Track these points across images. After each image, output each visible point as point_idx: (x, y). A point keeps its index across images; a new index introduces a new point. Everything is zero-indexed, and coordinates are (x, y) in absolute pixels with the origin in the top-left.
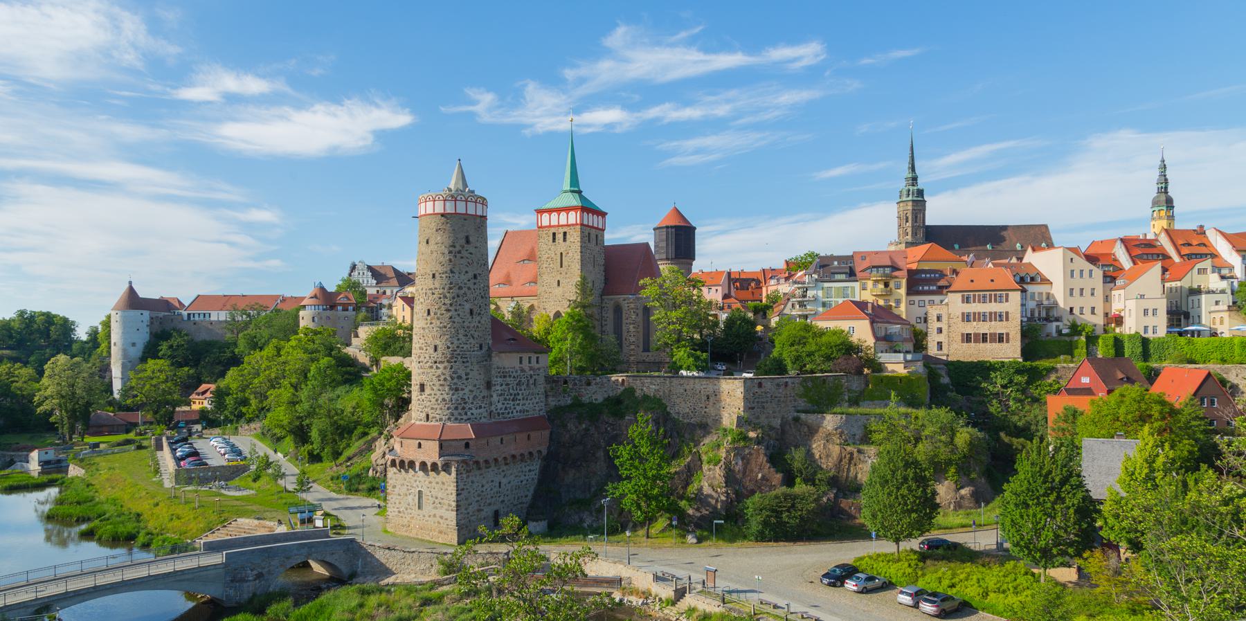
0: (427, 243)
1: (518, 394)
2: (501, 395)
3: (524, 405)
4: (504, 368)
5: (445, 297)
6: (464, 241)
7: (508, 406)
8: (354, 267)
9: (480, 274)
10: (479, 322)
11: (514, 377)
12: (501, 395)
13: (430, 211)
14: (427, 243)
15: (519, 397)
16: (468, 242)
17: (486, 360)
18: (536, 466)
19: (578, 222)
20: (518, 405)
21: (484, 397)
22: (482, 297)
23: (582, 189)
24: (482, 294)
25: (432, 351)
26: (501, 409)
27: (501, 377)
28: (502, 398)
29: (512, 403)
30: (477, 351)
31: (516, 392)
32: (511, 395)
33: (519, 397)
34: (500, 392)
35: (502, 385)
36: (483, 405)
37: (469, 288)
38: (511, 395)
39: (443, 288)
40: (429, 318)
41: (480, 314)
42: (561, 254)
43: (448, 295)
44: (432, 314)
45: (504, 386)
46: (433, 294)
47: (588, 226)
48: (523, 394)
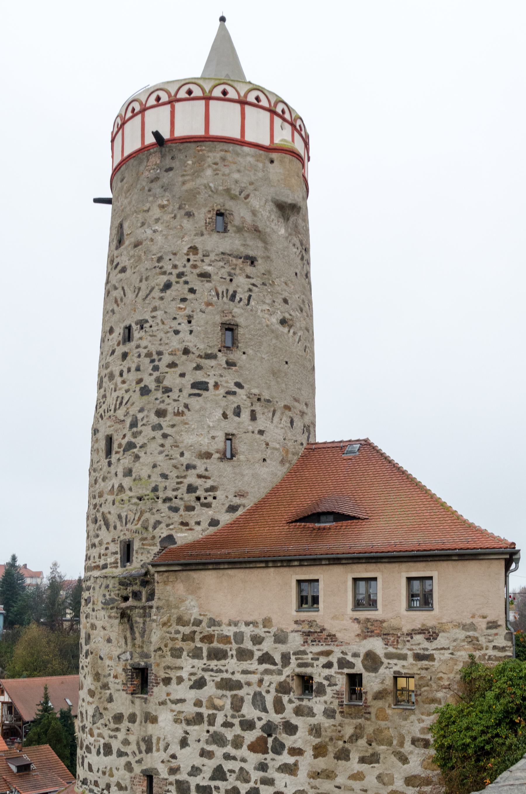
1: (291, 729)
2: (198, 719)
3: (329, 775)
4: (213, 623)
7: (227, 765)
9: (142, 324)
10: (128, 473)
11: (266, 658)
12: (198, 719)
15: (289, 741)
17: (136, 595)
20: (286, 769)
21: (118, 718)
22: (145, 391)
24: (149, 382)
26: (195, 771)
27: (196, 654)
28: (196, 731)
29: (254, 758)
30: (115, 564)
31: (276, 718)
32: (248, 725)
33: (289, 741)
34: (189, 709)
35: (200, 684)
36: (116, 745)
38: (248, 725)
41: (131, 446)
45: (210, 689)
48: (316, 730)
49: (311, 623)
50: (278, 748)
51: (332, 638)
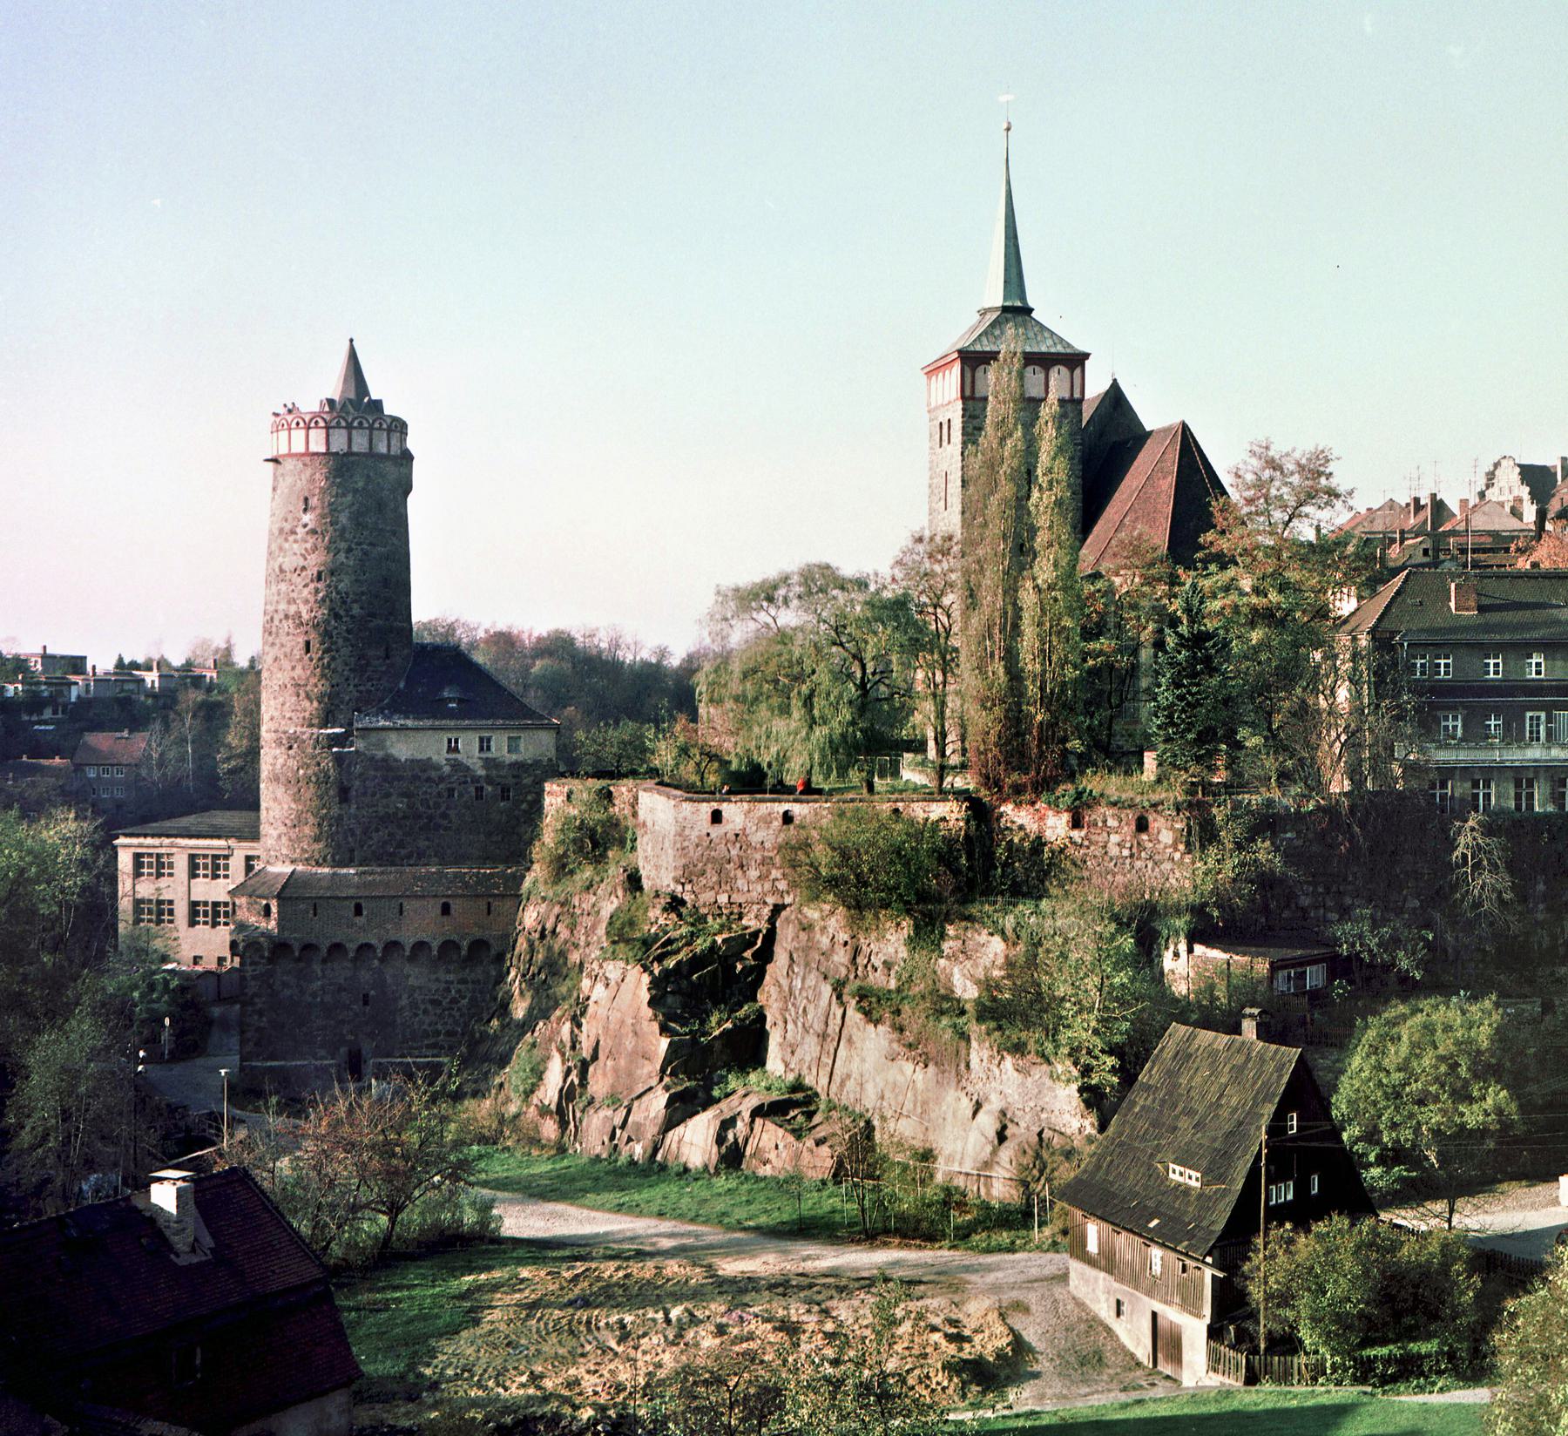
16: (305, 510)
23: (1031, 303)
37: (306, 602)
49: (456, 760)
50: (438, 827)
51: (468, 768)
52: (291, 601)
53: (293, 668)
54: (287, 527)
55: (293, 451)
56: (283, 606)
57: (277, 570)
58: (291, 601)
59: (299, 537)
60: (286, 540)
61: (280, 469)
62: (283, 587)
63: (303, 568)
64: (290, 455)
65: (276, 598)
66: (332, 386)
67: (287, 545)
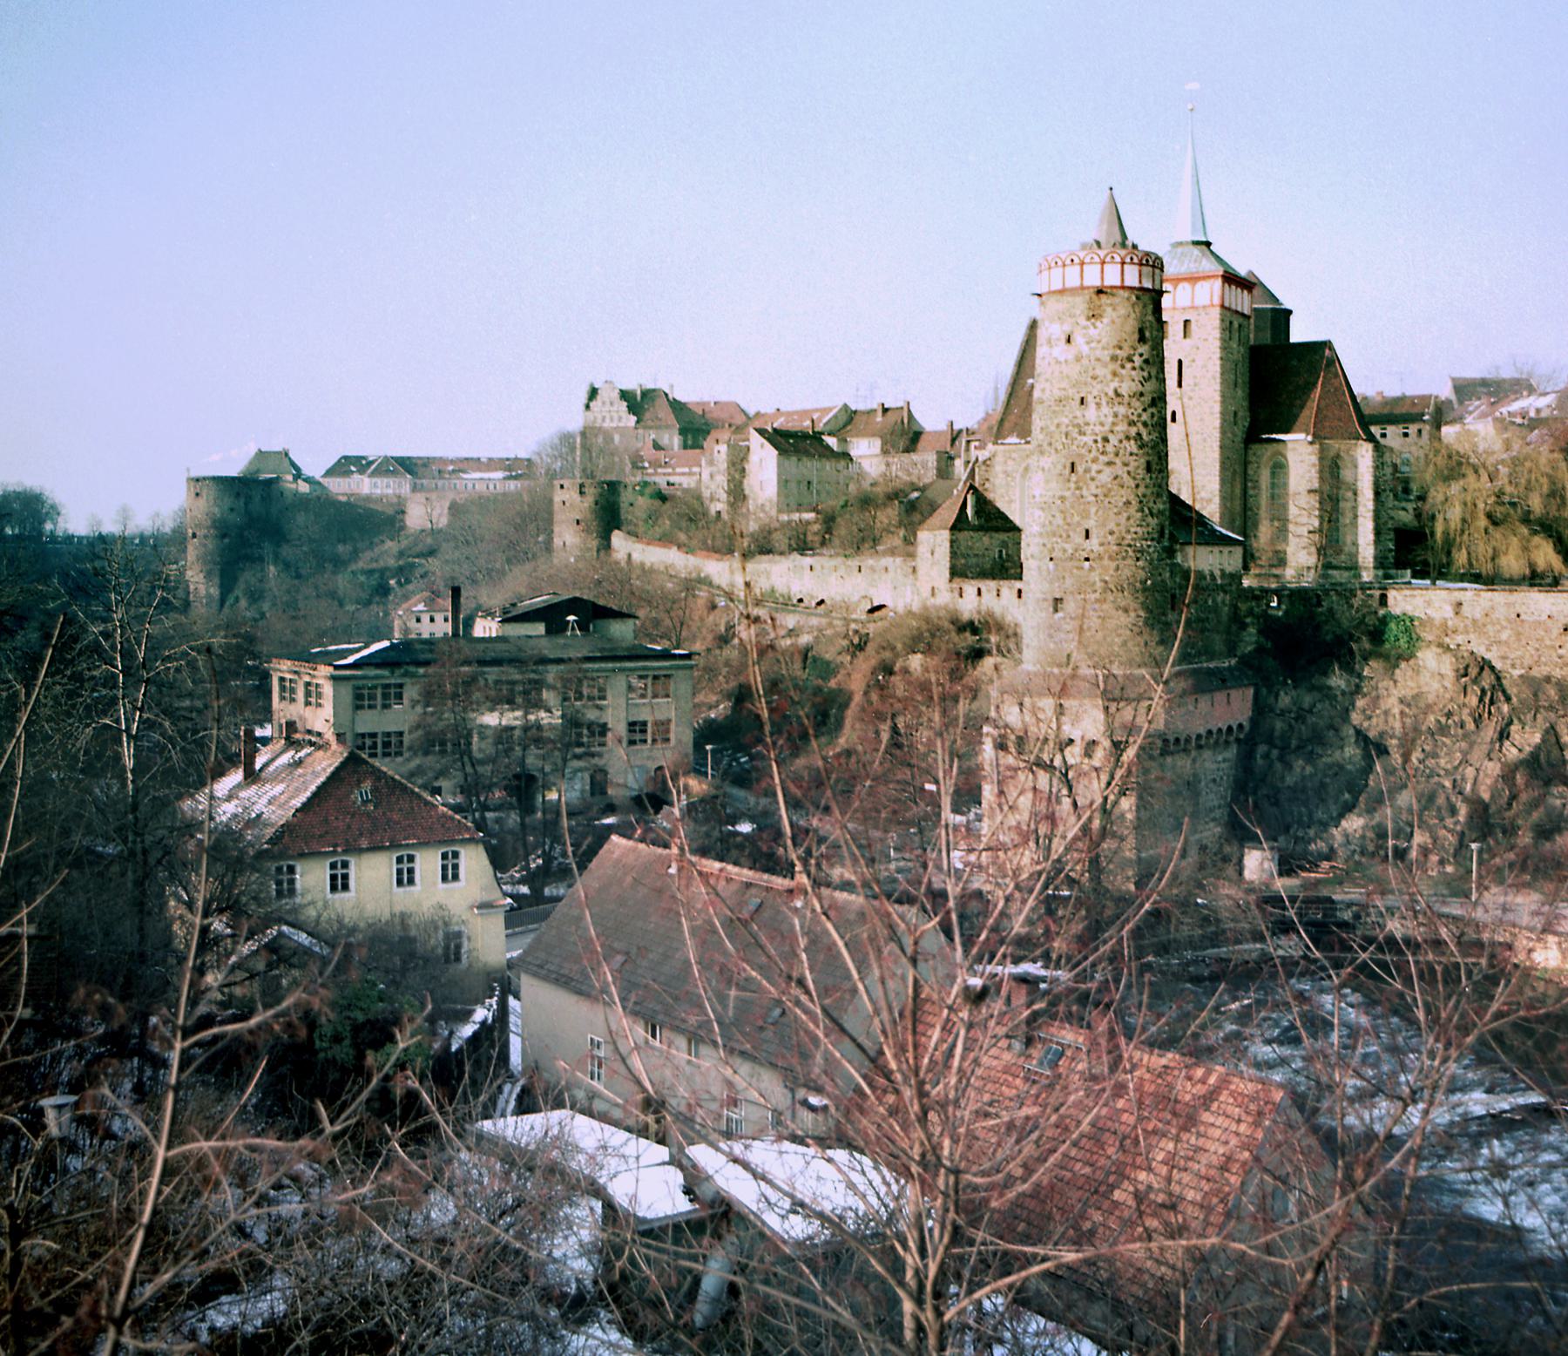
0: (1069, 341)
5: (1106, 440)
6: (1136, 336)
8: (593, 393)
13: (1073, 280)
14: (1069, 341)
18: (1232, 752)
19: (1217, 301)
25: (1079, 538)
37: (1145, 424)
39: (1102, 424)
40: (1074, 477)
42: (1180, 362)
43: (1111, 437)
44: (1080, 469)
46: (1082, 433)
47: (1229, 309)
52: (1132, 423)
53: (1137, 486)
54: (1122, 354)
55: (1127, 283)
56: (1122, 427)
57: (1111, 394)
58: (1132, 423)
59: (1137, 364)
60: (1123, 367)
61: (1104, 298)
62: (1122, 410)
63: (1142, 394)
64: (1123, 287)
65: (1111, 419)
66: (1093, 226)
67: (1124, 372)
